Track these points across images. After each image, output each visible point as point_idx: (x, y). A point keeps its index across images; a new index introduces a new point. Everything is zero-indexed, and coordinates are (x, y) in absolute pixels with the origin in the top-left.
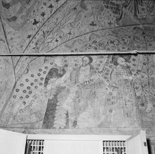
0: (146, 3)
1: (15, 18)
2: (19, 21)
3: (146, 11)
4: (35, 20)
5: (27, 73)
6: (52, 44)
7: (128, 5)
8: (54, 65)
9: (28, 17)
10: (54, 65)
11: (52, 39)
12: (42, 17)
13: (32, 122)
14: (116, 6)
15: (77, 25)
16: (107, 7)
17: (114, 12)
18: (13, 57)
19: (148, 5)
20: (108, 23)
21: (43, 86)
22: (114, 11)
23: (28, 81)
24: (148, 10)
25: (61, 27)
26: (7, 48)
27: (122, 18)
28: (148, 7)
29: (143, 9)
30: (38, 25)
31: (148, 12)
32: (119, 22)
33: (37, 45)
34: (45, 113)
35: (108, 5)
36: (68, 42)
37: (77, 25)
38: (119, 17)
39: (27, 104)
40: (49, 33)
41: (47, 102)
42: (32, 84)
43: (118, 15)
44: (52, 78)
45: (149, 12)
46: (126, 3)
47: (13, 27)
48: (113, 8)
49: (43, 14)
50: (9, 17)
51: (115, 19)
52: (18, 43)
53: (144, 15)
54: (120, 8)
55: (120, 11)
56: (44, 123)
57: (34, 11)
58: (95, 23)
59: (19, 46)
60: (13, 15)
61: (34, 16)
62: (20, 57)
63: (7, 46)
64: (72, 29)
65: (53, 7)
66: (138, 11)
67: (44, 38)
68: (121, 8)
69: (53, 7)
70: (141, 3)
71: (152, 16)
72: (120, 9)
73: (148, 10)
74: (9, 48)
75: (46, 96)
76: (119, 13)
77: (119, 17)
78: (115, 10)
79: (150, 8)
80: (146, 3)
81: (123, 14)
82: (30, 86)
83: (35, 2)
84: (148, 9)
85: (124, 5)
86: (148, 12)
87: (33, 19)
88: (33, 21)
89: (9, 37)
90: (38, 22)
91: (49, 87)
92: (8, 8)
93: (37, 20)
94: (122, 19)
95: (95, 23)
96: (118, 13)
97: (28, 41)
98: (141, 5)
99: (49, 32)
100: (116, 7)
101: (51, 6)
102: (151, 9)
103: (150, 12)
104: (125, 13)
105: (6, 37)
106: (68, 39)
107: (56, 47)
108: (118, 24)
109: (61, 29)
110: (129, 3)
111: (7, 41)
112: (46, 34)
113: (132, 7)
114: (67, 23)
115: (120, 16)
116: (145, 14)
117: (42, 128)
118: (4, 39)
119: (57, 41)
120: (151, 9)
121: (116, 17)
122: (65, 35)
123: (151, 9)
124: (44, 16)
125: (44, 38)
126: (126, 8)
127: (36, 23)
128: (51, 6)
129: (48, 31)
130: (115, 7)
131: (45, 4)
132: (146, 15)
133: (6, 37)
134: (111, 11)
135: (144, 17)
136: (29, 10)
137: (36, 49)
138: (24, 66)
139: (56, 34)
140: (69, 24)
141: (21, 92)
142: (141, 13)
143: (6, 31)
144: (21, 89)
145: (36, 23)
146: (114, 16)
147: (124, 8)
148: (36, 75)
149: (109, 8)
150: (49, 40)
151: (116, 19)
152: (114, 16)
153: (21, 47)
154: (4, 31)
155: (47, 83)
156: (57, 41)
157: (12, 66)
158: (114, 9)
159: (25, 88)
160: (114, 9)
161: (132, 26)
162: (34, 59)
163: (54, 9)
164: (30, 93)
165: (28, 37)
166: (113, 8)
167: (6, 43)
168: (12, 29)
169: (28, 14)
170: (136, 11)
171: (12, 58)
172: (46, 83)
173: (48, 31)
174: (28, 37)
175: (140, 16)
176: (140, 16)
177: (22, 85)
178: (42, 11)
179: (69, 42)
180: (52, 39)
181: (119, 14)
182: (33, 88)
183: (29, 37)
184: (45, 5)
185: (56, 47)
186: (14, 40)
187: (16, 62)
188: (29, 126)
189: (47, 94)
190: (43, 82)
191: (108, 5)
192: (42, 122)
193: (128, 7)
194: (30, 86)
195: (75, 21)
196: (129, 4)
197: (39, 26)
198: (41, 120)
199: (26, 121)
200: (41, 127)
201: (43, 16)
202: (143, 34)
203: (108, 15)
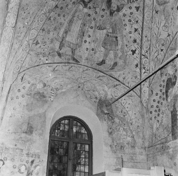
1: (115, 64)
2: (120, 62)
4: (132, 51)
5: (152, 93)
6: (160, 55)
8: (168, 75)
9: (125, 54)
10: (168, 75)
11: (157, 52)
12: (136, 44)
13: (165, 137)
15: (171, 22)
18: (134, 90)
21: (165, 100)
23: (155, 101)
25: (158, 36)
26: (125, 86)
30: (137, 52)
33: (146, 69)
34: (171, 126)
36: (171, 45)
37: (171, 22)
39: (160, 122)
40: (148, 52)
41: (170, 115)
42: (158, 102)
44: (169, 89)
47: (119, 70)
49: (135, 41)
50: (111, 67)
52: (131, 77)
56: (173, 135)
57: (127, 45)
59: (134, 78)
60: (112, 63)
61: (129, 48)
62: (139, 85)
63: (124, 86)
64: (169, 30)
65: (138, 29)
67: (148, 58)
69: (138, 29)
74: (126, 86)
75: (169, 109)
82: (158, 104)
83: (123, 38)
87: (130, 51)
88: (131, 53)
89: (121, 79)
90: (135, 50)
91: (169, 100)
92: (105, 63)
93: (134, 49)
97: (138, 70)
99: (147, 51)
101: (136, 30)
105: (119, 81)
106: (170, 42)
107: (165, 56)
109: (160, 38)
111: (122, 83)
112: (147, 55)
114: (161, 28)
117: (173, 140)
118: (117, 83)
119: (162, 50)
122: (165, 41)
124: (137, 42)
125: (148, 58)
127: (134, 52)
128: (136, 30)
129: (146, 51)
131: (130, 33)
133: (119, 81)
136: (121, 48)
137: (147, 72)
138: (145, 92)
139: (157, 45)
140: (164, 28)
141: (154, 113)
143: (116, 77)
144: (153, 110)
145: (134, 52)
148: (159, 92)
150: (156, 54)
153: (136, 78)
154: (115, 78)
155: (167, 96)
156: (162, 50)
157: (137, 96)
159: (155, 108)
162: (153, 79)
163: (140, 30)
164: (159, 110)
165: (136, 67)
167: (122, 84)
168: (119, 73)
169: (123, 52)
171: (134, 91)
172: (167, 96)
173: (146, 51)
174: (136, 67)
177: (152, 106)
178: (132, 39)
179: (172, 44)
180: (157, 52)
182: (160, 105)
183: (137, 66)
184: (131, 33)
185: (165, 56)
186: (126, 78)
187: (139, 92)
188: (164, 141)
189: (169, 107)
190: (165, 96)
192: (171, 135)
194: (158, 104)
195: (167, 20)
197: (138, 52)
198: (170, 133)
199: (162, 137)
200: (171, 139)
201: (136, 42)
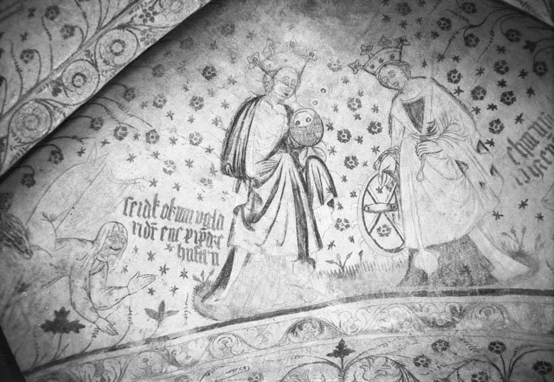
0: (353, 195)
3: (357, 231)
7: (264, 212)
16: (148, 233)
17: (183, 254)
19: (368, 201)
20: (148, 311)
22: (184, 245)
29: (341, 225)
31: (369, 234)
35: (151, 220)
38: (213, 279)
43: (207, 268)
45: (375, 234)
46: (249, 206)
48: (182, 234)
51: (187, 287)
53: (350, 255)
54: (216, 233)
55: (218, 244)
58: (72, 318)
66: (318, 236)
68: (226, 233)
71: (391, 251)
72: (221, 237)
76: (215, 255)
77: (211, 273)
79: (380, 213)
80: (353, 195)
81: (239, 258)
85: (243, 213)
94: (228, 286)
95: (72, 318)
96: (209, 258)
98: (331, 204)
100: (198, 228)
102: (383, 215)
104: (248, 256)
110: (265, 202)
113: (287, 221)
115: (218, 270)
116: (355, 248)
121: (196, 279)
130: (189, 232)
132: (361, 253)
134: (169, 248)
135: (350, 263)
146: (184, 275)
149: (157, 234)
151: (197, 289)
152: (184, 275)
158: (187, 238)
170: (306, 236)
175: (331, 262)
176: (331, 262)
191: (151, 220)
193: (266, 220)
196: (266, 207)
202: (336, 354)
203: (153, 268)
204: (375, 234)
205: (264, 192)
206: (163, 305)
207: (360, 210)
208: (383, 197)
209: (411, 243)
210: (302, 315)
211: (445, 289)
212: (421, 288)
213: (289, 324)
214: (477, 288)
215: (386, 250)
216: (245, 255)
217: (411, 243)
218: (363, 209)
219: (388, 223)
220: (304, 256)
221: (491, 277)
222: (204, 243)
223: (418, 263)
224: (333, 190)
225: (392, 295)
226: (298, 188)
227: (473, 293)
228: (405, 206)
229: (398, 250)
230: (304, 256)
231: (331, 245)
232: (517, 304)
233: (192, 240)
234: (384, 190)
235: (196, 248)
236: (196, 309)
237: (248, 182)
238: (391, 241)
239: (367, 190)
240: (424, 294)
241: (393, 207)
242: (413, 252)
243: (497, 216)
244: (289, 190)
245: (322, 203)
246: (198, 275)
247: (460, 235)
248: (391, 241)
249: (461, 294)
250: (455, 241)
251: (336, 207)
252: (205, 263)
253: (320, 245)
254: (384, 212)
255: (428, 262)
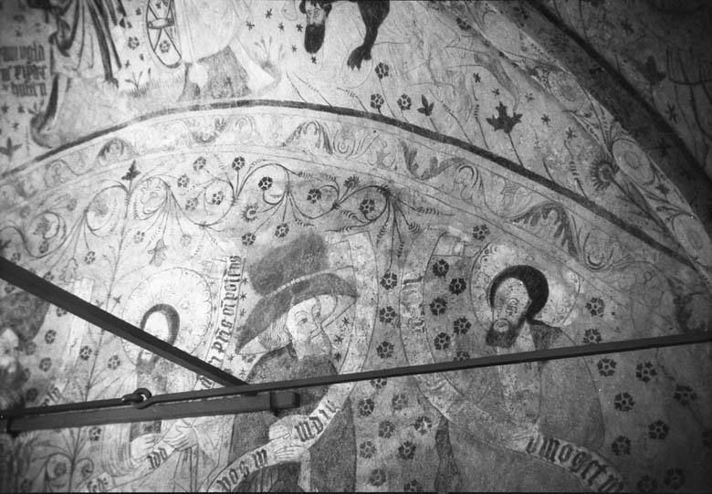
3: (144, 48)
7: (73, 37)
14: (22, 57)
19: (151, 17)
22: (16, 82)
24: (154, 43)
27: (59, 105)
28: (149, 25)
29: (133, 43)
31: (154, 50)
32: (44, 131)
38: (44, 109)
43: (37, 100)
45: (158, 50)
46: (60, 34)
48: (12, 73)
53: (141, 73)
54: (40, 64)
55: (43, 74)
68: (47, 62)
70: (119, 17)
71: (171, 67)
72: (44, 67)
73: (154, 43)
76: (42, 85)
77: (42, 104)
78: (22, 80)
79: (160, 29)
80: (138, 12)
81: (62, 85)
84: (154, 33)
86: (154, 50)
96: (38, 89)
98: (122, 24)
100: (23, 62)
102: (163, 30)
103: (163, 51)
108: (41, 144)
115: (47, 99)
116: (144, 66)
120: (164, 37)
121: (31, 112)
123: (164, 37)
126: (67, 55)
130: (18, 68)
132: (149, 70)
142: (128, 64)
147: (58, 56)
151: (33, 122)
158: (17, 75)
160: (17, 75)
161: (95, 141)
166: (12, 73)
175: (128, 81)
176: (128, 81)
181: (43, 94)
193: (76, 46)
204: (158, 50)
205: (69, 18)
206: (9, 141)
207: (145, 27)
208: (162, 13)
209: (186, 58)
210: (111, 135)
211: (213, 101)
212: (195, 103)
213: (101, 147)
214: (236, 99)
215: (168, 66)
216: (66, 80)
217: (186, 58)
218: (148, 26)
219: (168, 39)
220: (109, 77)
221: (247, 88)
222: (32, 77)
223: (192, 78)
224: (122, 10)
225: (172, 111)
226: (94, 10)
227: (233, 105)
228: (180, 20)
229: (177, 65)
230: (109, 77)
231: (128, 64)
232: (263, 115)
233: (21, 76)
234: (162, 5)
235: (26, 82)
236: (35, 140)
237: (53, 11)
238: (171, 57)
239: (149, 7)
240: (196, 108)
241: (171, 22)
242: (188, 65)
243: (250, 26)
244: (88, 14)
245: (115, 24)
246: (32, 107)
247: (223, 46)
248: (171, 57)
249: (225, 106)
250: (220, 53)
251: (127, 26)
252: (36, 95)
253: (119, 65)
254: (164, 27)
255: (200, 76)
